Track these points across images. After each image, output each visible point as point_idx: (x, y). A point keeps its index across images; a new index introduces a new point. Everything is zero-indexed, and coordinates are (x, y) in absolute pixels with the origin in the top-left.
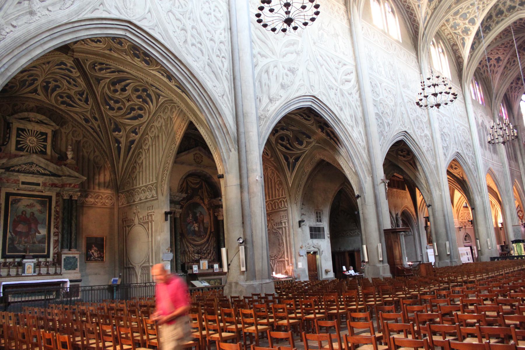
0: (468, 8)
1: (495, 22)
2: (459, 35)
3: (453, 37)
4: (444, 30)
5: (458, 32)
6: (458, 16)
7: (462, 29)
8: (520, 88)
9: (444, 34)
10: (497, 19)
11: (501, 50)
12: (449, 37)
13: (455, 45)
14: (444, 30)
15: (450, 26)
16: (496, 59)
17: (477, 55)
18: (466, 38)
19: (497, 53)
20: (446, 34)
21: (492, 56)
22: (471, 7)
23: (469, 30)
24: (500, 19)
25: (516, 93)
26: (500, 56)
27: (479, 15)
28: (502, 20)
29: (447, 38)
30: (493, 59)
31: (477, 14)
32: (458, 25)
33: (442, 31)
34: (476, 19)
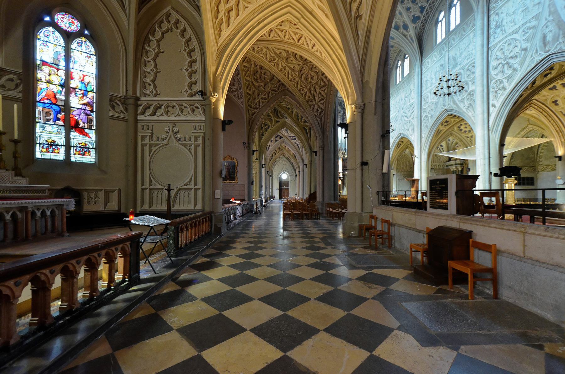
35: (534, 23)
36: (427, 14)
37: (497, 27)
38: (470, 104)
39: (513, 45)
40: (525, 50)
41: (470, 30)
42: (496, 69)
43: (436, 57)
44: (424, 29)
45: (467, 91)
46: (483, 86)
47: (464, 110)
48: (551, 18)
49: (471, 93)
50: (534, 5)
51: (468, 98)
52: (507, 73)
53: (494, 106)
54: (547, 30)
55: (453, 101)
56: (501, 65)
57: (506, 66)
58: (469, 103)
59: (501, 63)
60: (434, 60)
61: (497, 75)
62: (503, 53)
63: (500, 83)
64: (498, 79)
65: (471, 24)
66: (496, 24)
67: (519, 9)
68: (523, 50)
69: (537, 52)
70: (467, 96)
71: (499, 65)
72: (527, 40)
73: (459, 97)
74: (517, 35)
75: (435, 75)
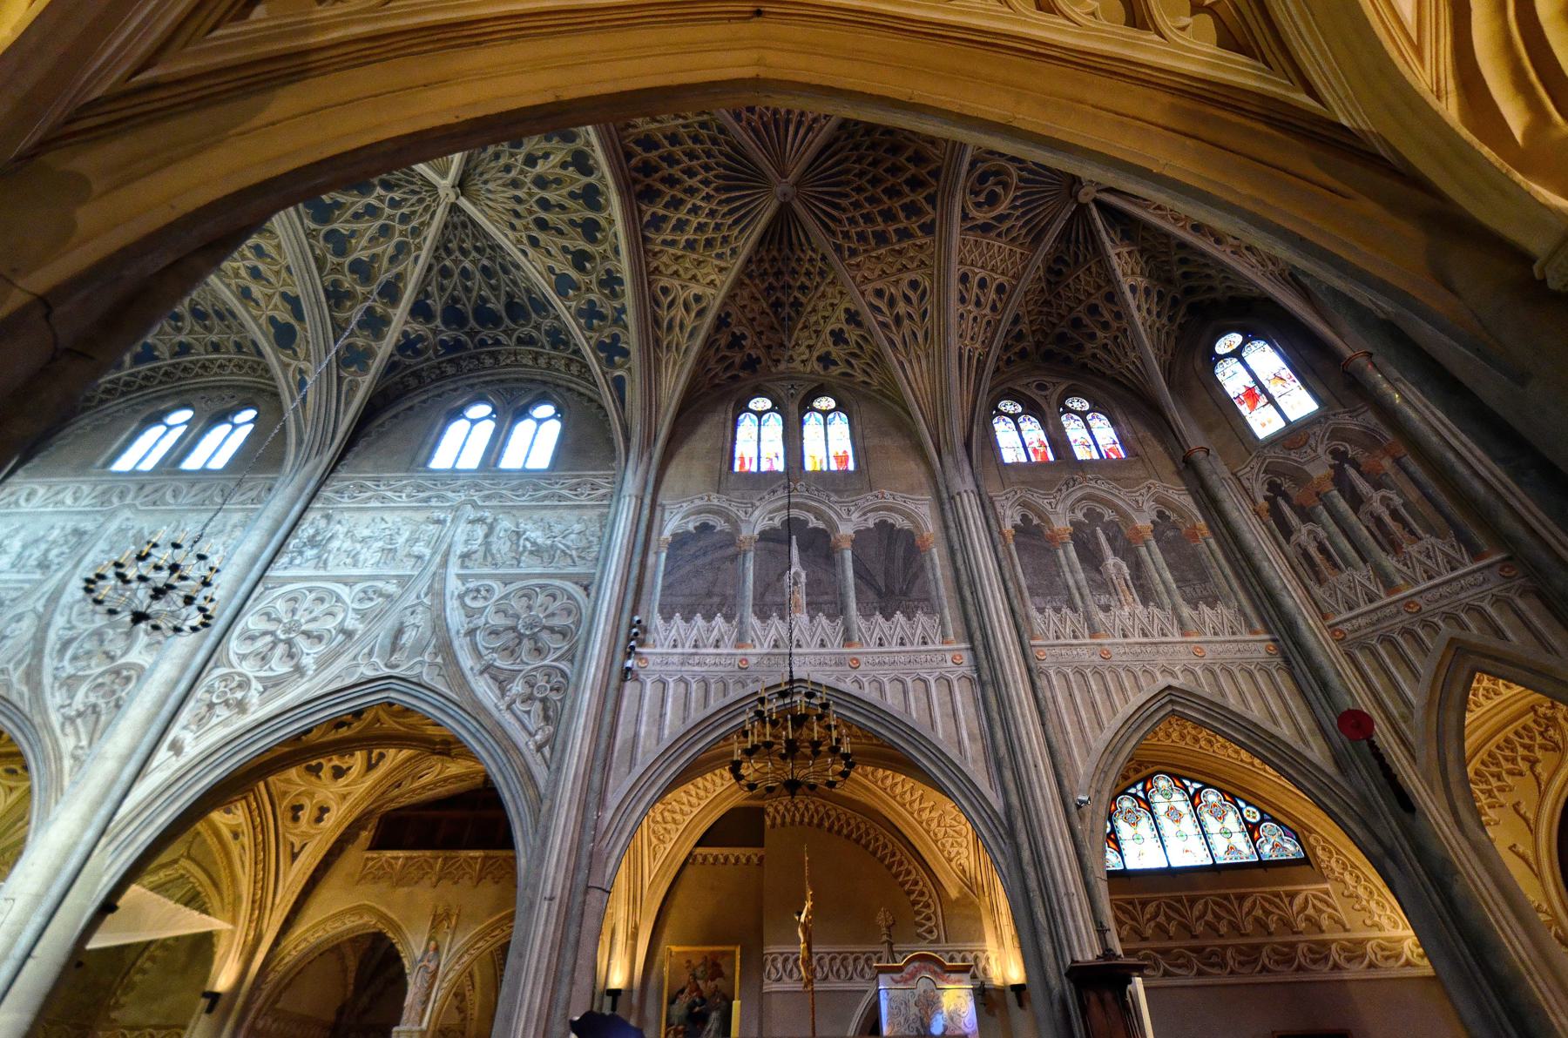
1: (611, 255)
8: (1125, 330)
10: (606, 246)
11: (829, 290)
14: (549, 363)
16: (848, 321)
19: (832, 305)
20: (563, 369)
21: (833, 320)
25: (1132, 355)
26: (843, 307)
29: (572, 375)
30: (845, 327)
35: (391, 588)
36: (146, 378)
37: (312, 542)
38: (94, 706)
39: (326, 605)
40: (349, 634)
41: (242, 503)
42: (248, 642)
43: (76, 499)
44: (102, 401)
45: (112, 658)
46: (184, 668)
47: (55, 719)
48: (427, 601)
49: (125, 673)
50: (409, 555)
51: (101, 685)
52: (273, 666)
53: (176, 748)
54: (410, 620)
55: (29, 666)
56: (268, 639)
57: (281, 649)
58: (92, 699)
59: (272, 633)
60: (63, 503)
61: (243, 657)
62: (294, 612)
63: (240, 686)
64: (239, 670)
65: (253, 494)
66: (314, 536)
67: (377, 540)
68: (343, 631)
69: (370, 654)
70: (102, 674)
71: (265, 633)
72: (362, 615)
73: (66, 663)
74: (347, 589)
75: (24, 547)
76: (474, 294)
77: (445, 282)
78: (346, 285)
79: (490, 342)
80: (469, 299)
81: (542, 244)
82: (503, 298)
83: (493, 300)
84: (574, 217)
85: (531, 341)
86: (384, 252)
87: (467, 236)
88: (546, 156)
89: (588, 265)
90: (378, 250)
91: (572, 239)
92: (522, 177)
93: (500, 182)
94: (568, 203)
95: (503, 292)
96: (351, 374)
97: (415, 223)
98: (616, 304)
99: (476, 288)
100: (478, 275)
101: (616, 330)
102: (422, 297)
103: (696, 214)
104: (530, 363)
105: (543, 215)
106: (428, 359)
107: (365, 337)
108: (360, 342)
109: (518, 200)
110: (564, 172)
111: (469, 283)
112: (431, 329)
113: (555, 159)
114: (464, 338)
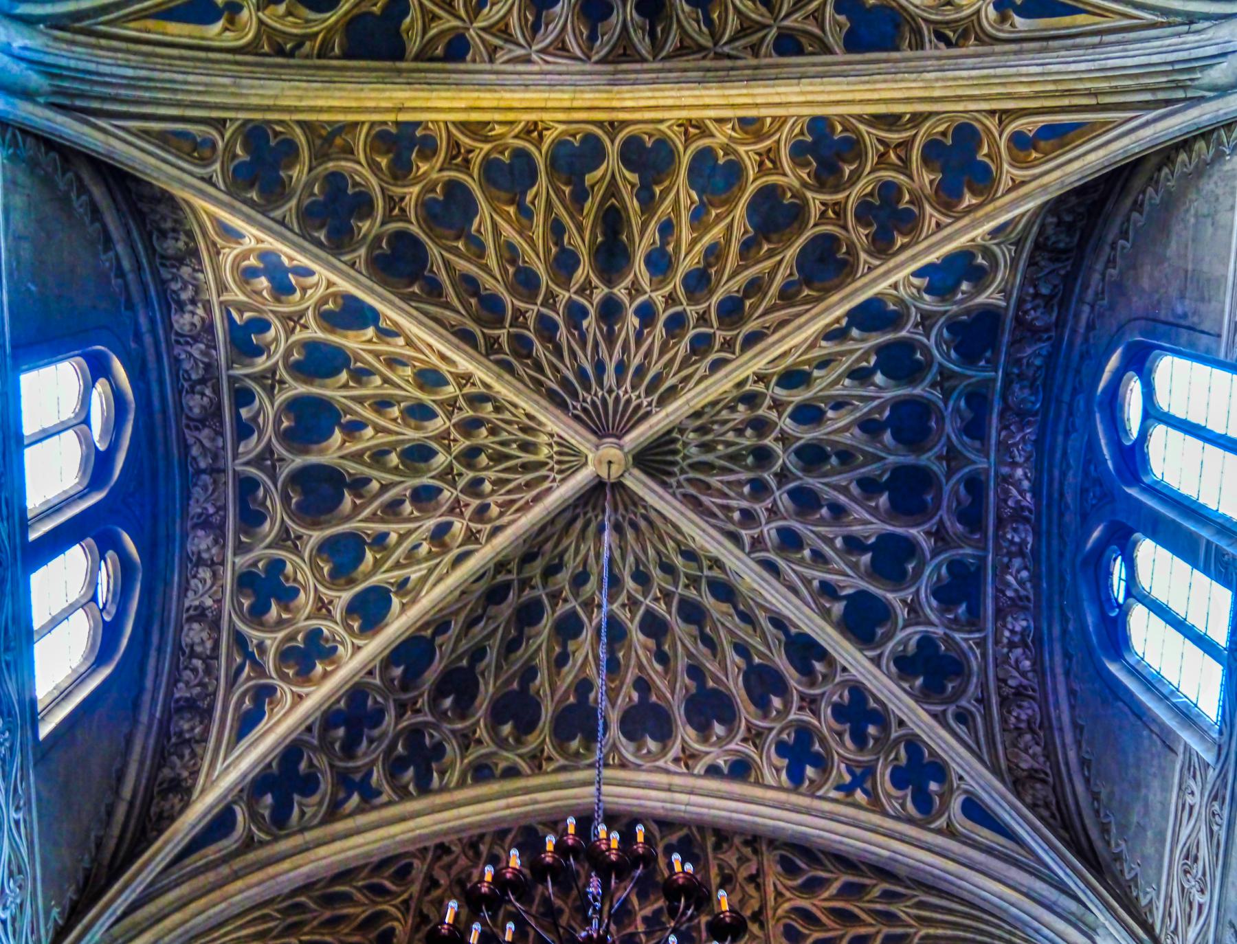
0: (392, 509)
1: (474, 753)
2: (259, 669)
3: (215, 655)
4: (200, 562)
5: (261, 646)
6: (316, 536)
7: (291, 637)
9: (185, 589)
10: (489, 747)
12: (196, 634)
13: (200, 709)
14: (200, 562)
15: (242, 561)
17: (286, 865)
18: (286, 691)
20: (191, 600)
22: (408, 508)
23: (329, 654)
24: (509, 757)
27: (424, 579)
28: (512, 772)
29: (179, 629)
31: (415, 573)
32: (287, 596)
33: (186, 558)
34: (396, 602)
76: (368, 414)
77: (408, 371)
78: (424, 167)
79: (245, 413)
80: (360, 400)
81: (492, 610)
82: (353, 468)
83: (352, 447)
84: (541, 679)
85: (251, 518)
86: (486, 269)
87: (502, 443)
88: (662, 658)
89: (448, 702)
90: (492, 261)
91: (499, 668)
92: (623, 598)
93: (617, 554)
94: (569, 676)
95: (367, 471)
96: (229, 146)
97: (539, 349)
98: (377, 776)
99: (382, 422)
100: (411, 434)
101: (326, 784)
102: (382, 324)
103: (544, 915)
104: (195, 509)
105: (547, 622)
106: (222, 288)
107: (309, 185)
108: (298, 174)
109: (580, 580)
110: (629, 678)
111: (395, 412)
112: (301, 314)
113: (655, 670)
114: (262, 363)
